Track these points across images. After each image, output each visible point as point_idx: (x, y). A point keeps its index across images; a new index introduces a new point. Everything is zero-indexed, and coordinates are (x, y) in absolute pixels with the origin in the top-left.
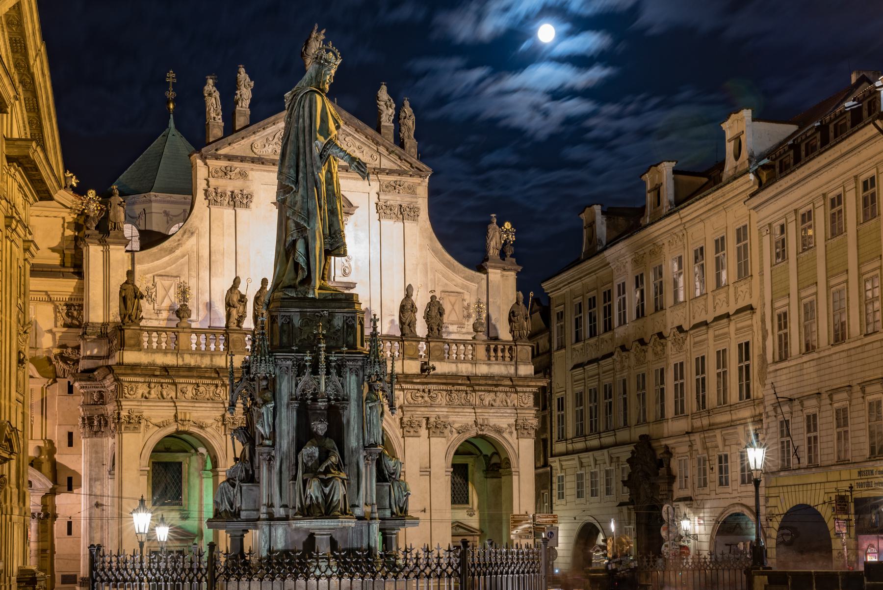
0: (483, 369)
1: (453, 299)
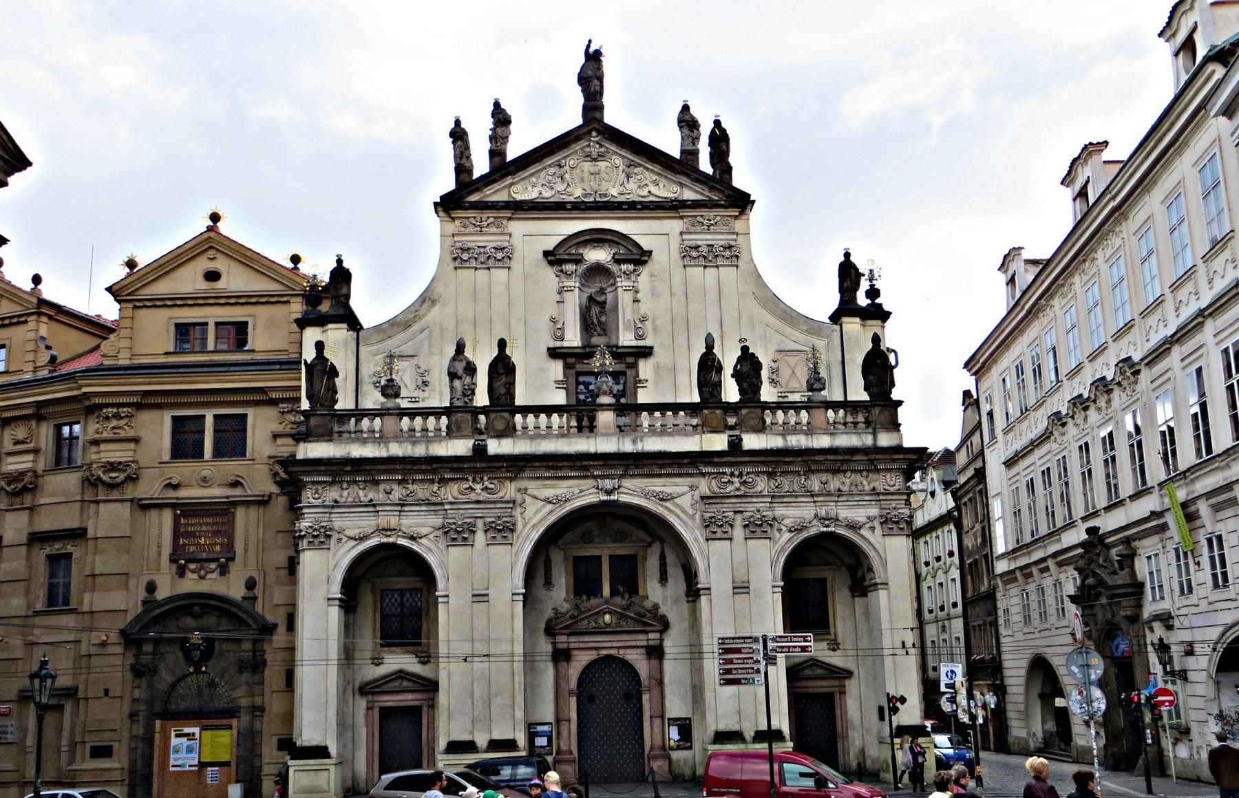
0: (823, 442)
1: (792, 360)
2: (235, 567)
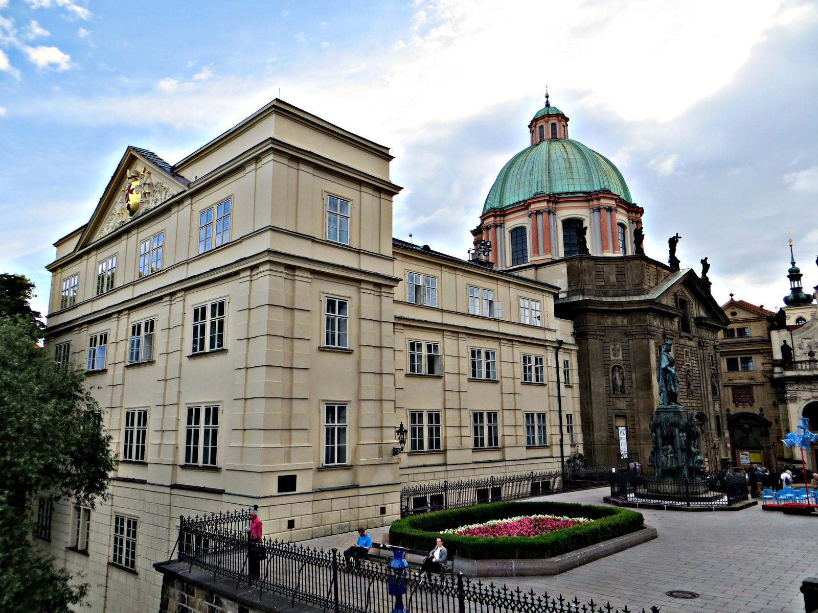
2: (755, 405)
